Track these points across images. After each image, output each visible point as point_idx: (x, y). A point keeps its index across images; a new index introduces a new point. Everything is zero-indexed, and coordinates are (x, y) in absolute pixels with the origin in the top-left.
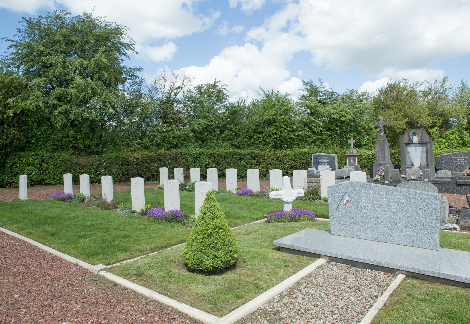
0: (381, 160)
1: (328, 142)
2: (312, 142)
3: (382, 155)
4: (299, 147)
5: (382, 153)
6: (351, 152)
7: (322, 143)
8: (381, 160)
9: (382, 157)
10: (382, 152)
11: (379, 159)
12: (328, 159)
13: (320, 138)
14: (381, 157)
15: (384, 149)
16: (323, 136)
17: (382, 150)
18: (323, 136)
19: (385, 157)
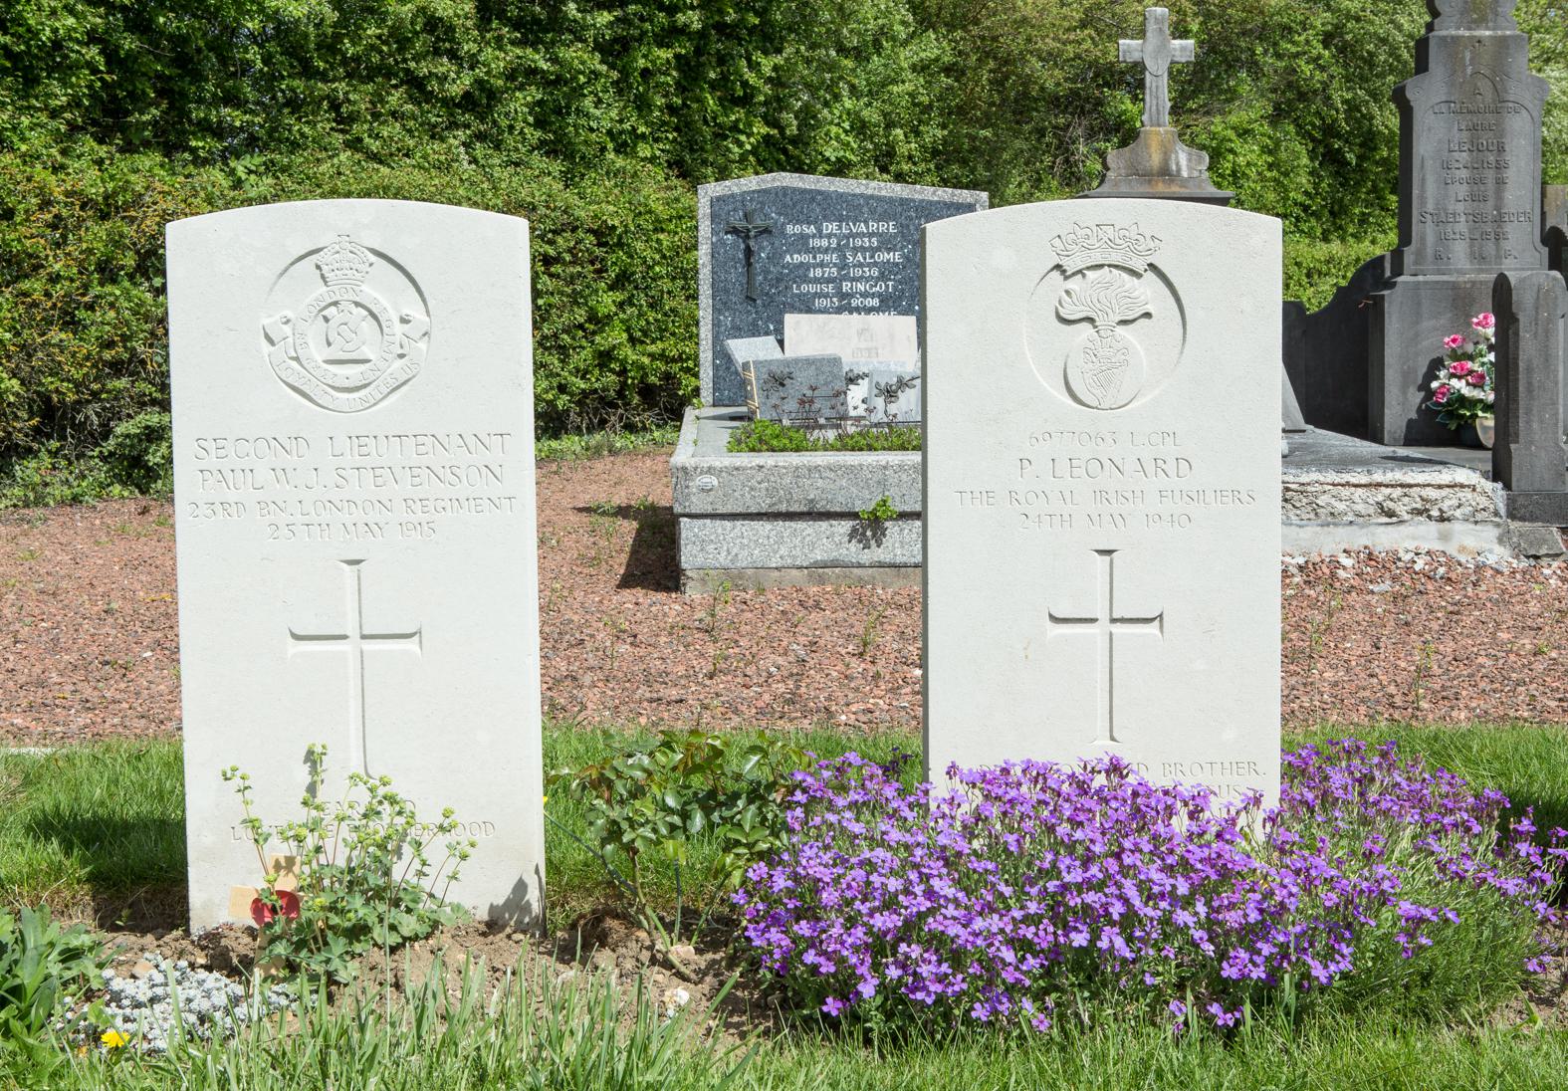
0: (1460, 251)
1: (603, 113)
2: (468, 101)
3: (1474, 198)
4: (355, 144)
5: (1475, 182)
6: (1155, 160)
7: (540, 124)
8: (1460, 251)
9: (1476, 219)
10: (1476, 167)
11: (1443, 239)
12: (887, 244)
13: (532, 72)
14: (1462, 226)
15: (1499, 132)
16: (563, 53)
17: (1476, 148)
18: (563, 53)
19: (1499, 220)
